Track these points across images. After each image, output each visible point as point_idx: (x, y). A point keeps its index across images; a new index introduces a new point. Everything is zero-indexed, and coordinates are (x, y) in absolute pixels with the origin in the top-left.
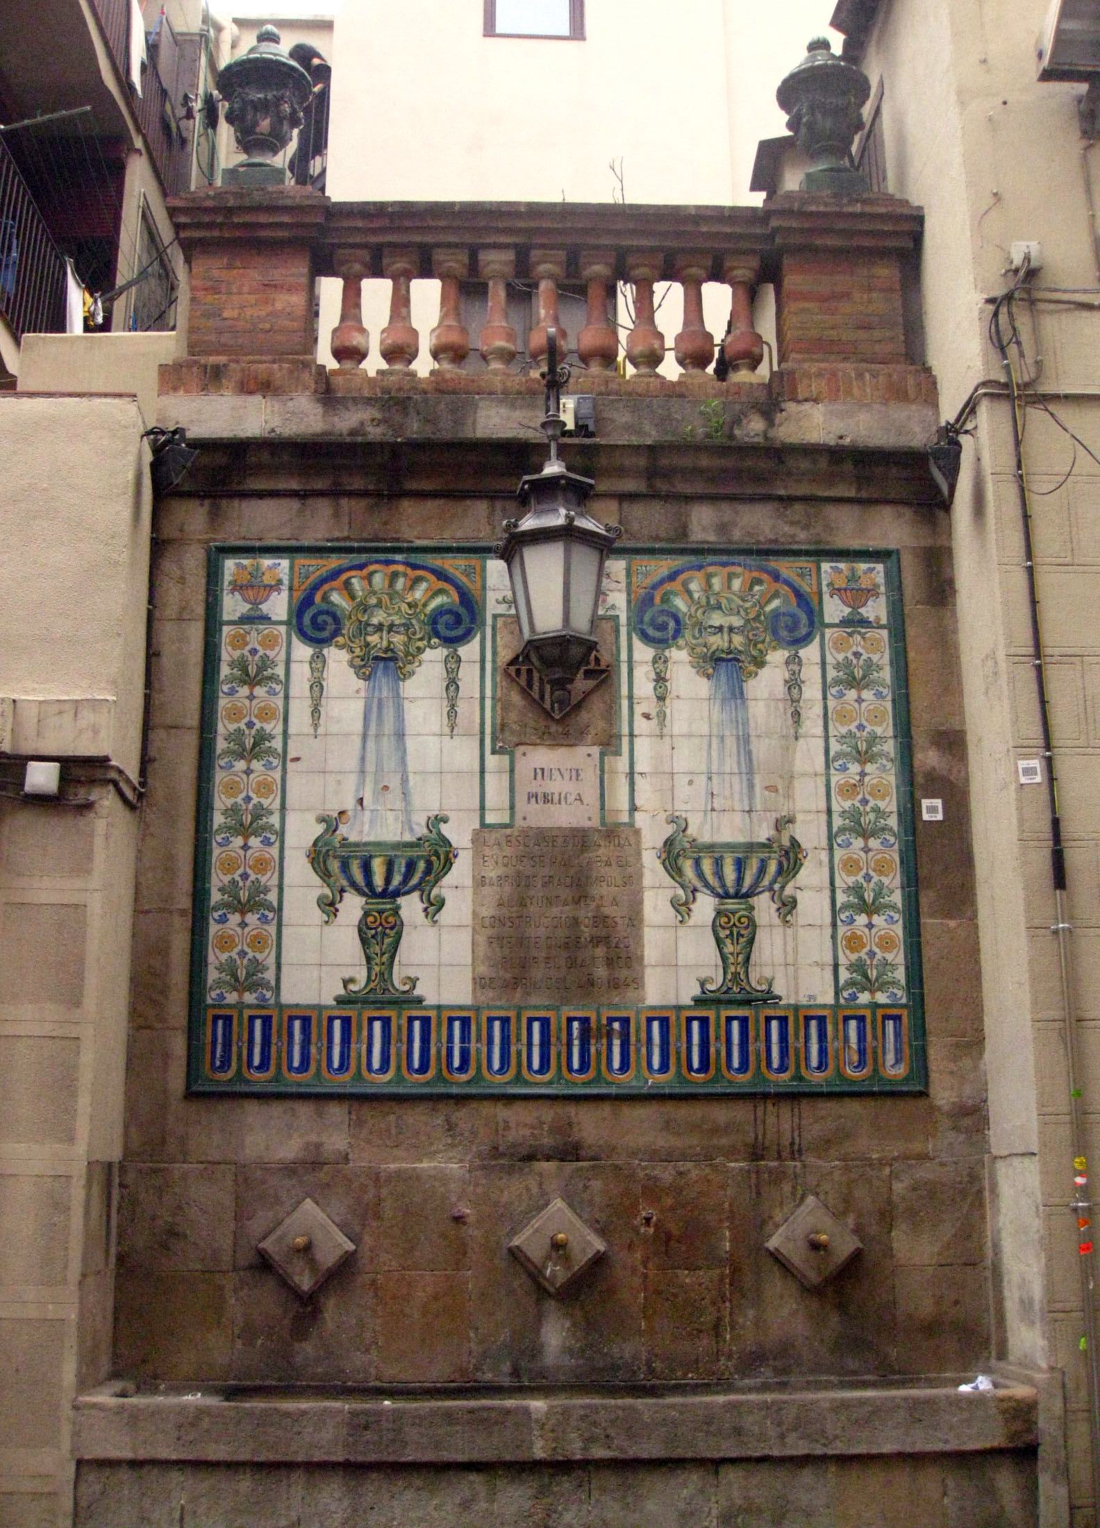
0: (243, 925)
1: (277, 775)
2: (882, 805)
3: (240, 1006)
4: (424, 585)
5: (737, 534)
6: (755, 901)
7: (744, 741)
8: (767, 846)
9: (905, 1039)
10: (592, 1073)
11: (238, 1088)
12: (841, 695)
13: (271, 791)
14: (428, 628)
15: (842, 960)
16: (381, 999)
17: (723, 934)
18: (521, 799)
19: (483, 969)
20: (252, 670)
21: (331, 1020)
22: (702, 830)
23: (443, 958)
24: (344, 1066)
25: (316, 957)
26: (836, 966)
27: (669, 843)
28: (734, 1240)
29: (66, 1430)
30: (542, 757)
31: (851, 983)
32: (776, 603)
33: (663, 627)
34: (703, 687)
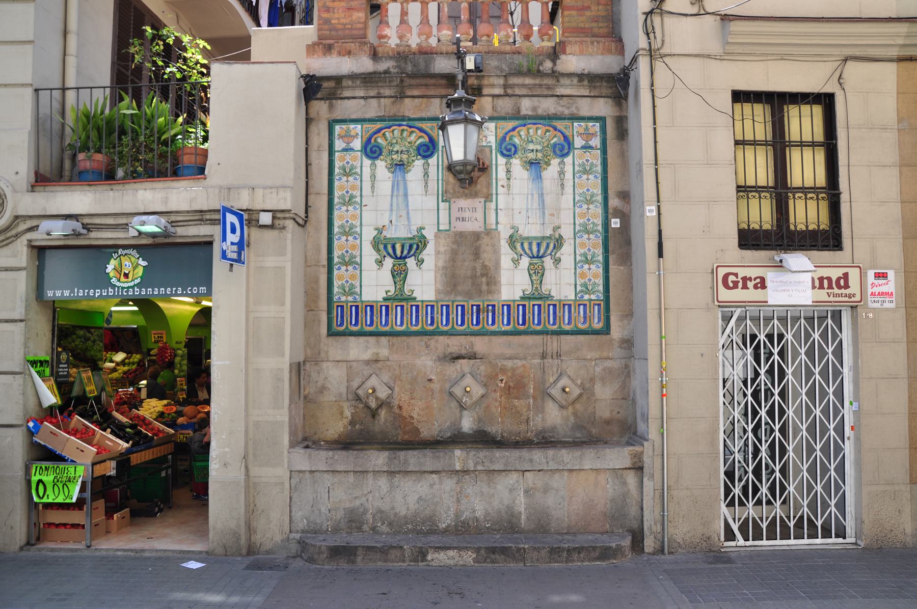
1: (358, 212)
2: (596, 221)
3: (347, 302)
5: (540, 112)
6: (544, 259)
7: (541, 195)
8: (550, 238)
9: (602, 313)
12: (581, 177)
15: (578, 282)
16: (400, 299)
17: (532, 272)
21: (381, 306)
23: (424, 283)
26: (576, 285)
27: (511, 237)
28: (534, 388)
29: (286, 460)
30: (463, 203)
31: (581, 291)
32: (555, 140)
34: (525, 174)
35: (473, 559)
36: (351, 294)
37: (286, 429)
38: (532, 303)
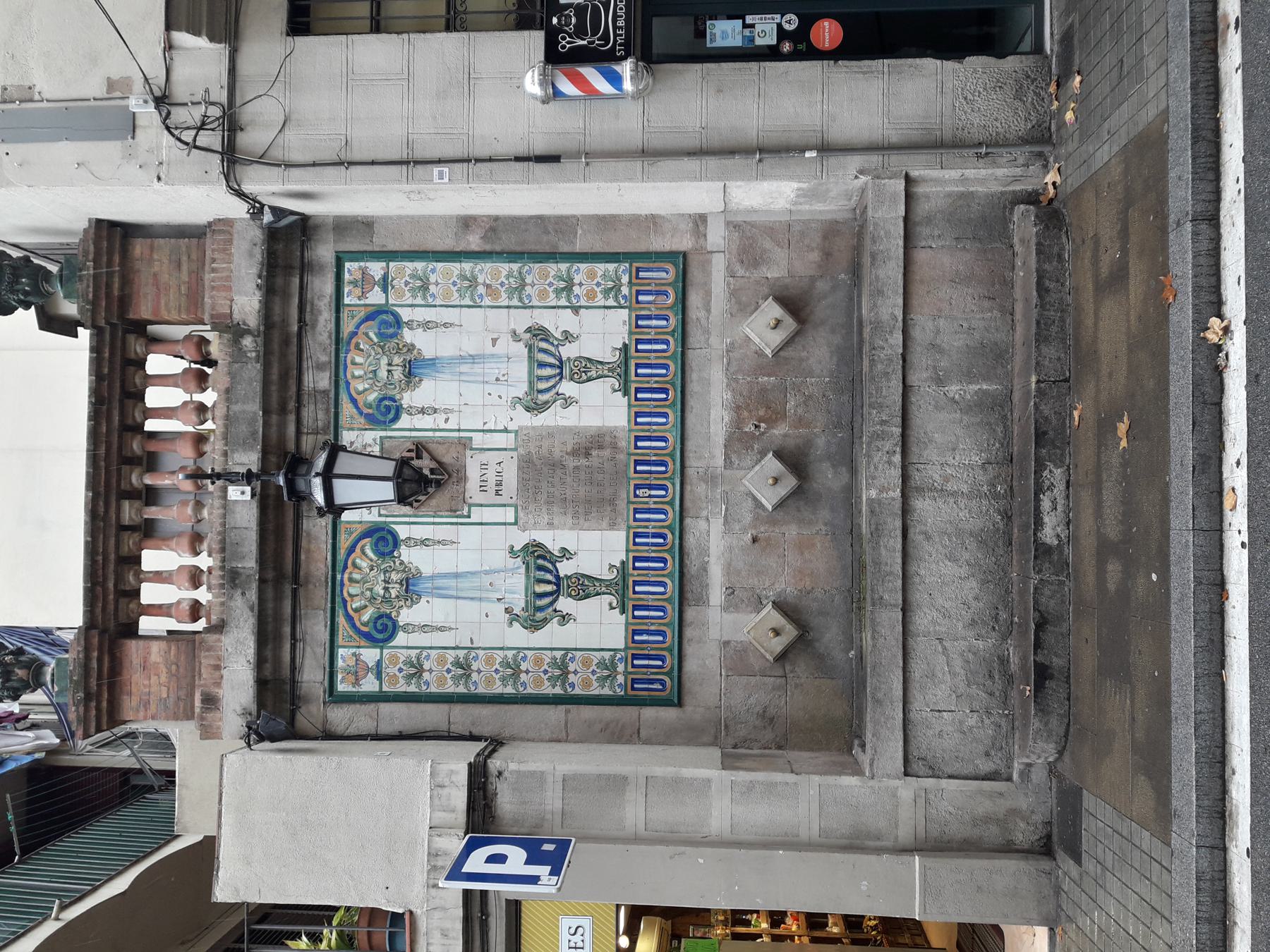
0: (575, 672)
1: (481, 653)
2: (504, 273)
3: (626, 673)
4: (358, 561)
8: (530, 348)
9: (651, 265)
10: (668, 459)
11: (676, 673)
12: (433, 295)
13: (492, 657)
14: (387, 558)
15: (601, 303)
16: (622, 587)
17: (584, 377)
18: (499, 500)
19: (605, 524)
20: (413, 671)
21: (634, 617)
22: (521, 389)
23: (597, 549)
24: (662, 609)
25: (597, 627)
27: (528, 409)
28: (769, 375)
31: (616, 299)
32: (372, 335)
33: (388, 409)
34: (427, 385)
35: (1057, 467)
36: (612, 666)
37: (831, 779)
38: (633, 378)
